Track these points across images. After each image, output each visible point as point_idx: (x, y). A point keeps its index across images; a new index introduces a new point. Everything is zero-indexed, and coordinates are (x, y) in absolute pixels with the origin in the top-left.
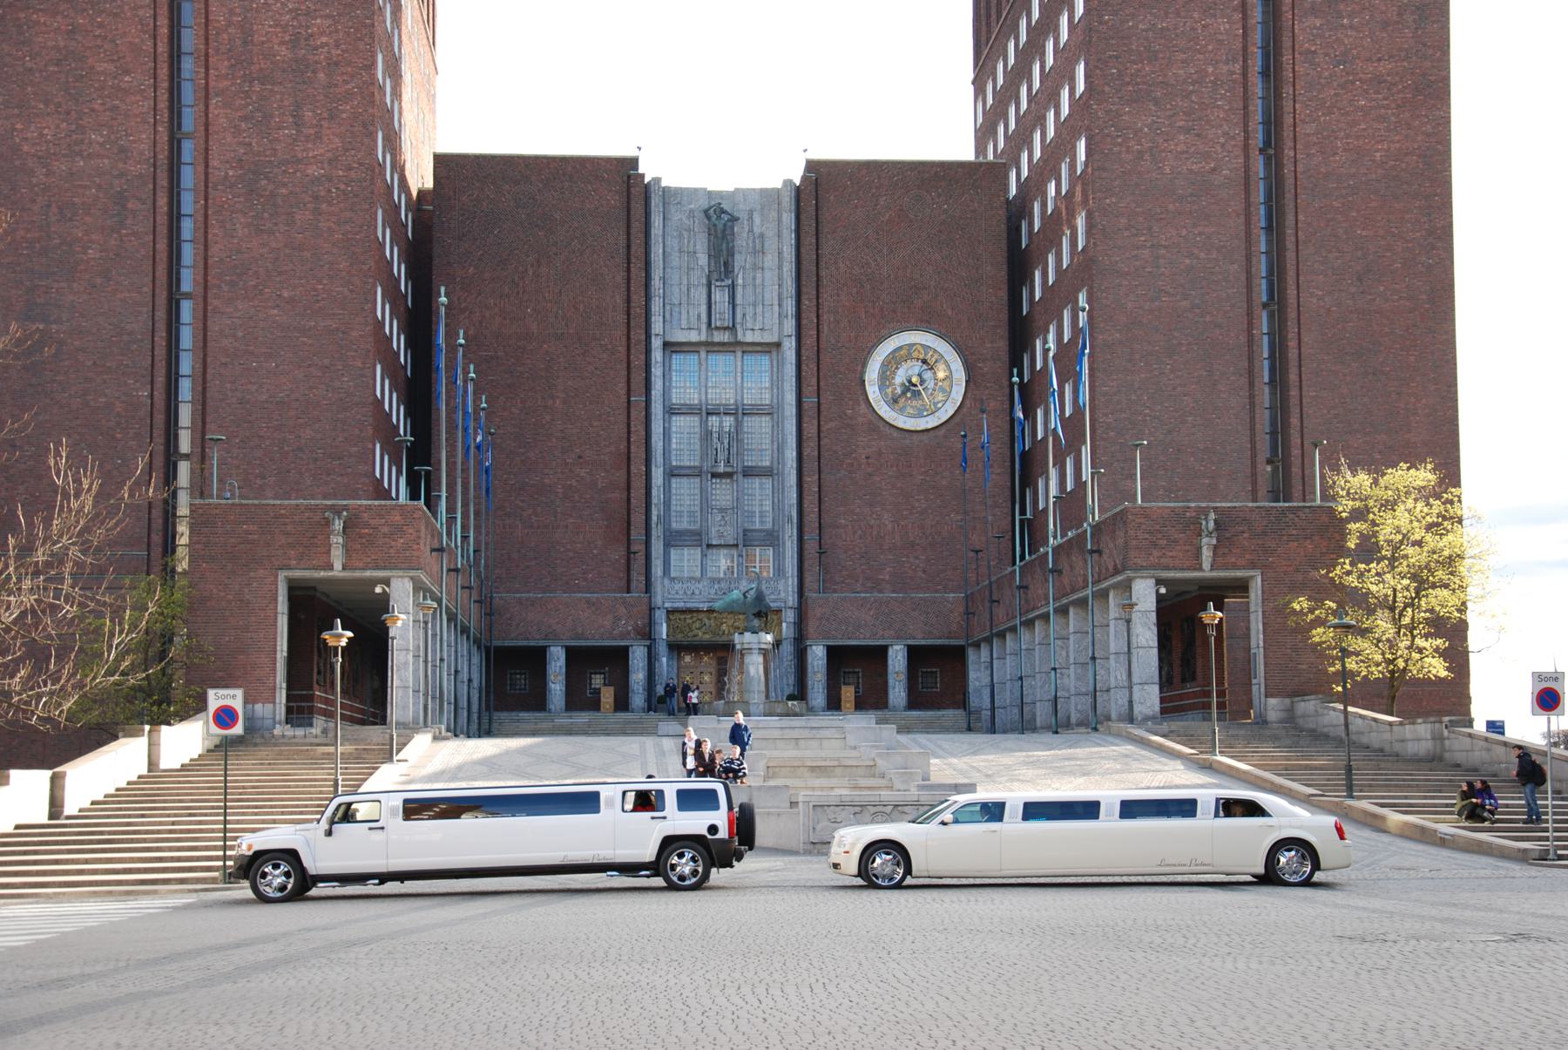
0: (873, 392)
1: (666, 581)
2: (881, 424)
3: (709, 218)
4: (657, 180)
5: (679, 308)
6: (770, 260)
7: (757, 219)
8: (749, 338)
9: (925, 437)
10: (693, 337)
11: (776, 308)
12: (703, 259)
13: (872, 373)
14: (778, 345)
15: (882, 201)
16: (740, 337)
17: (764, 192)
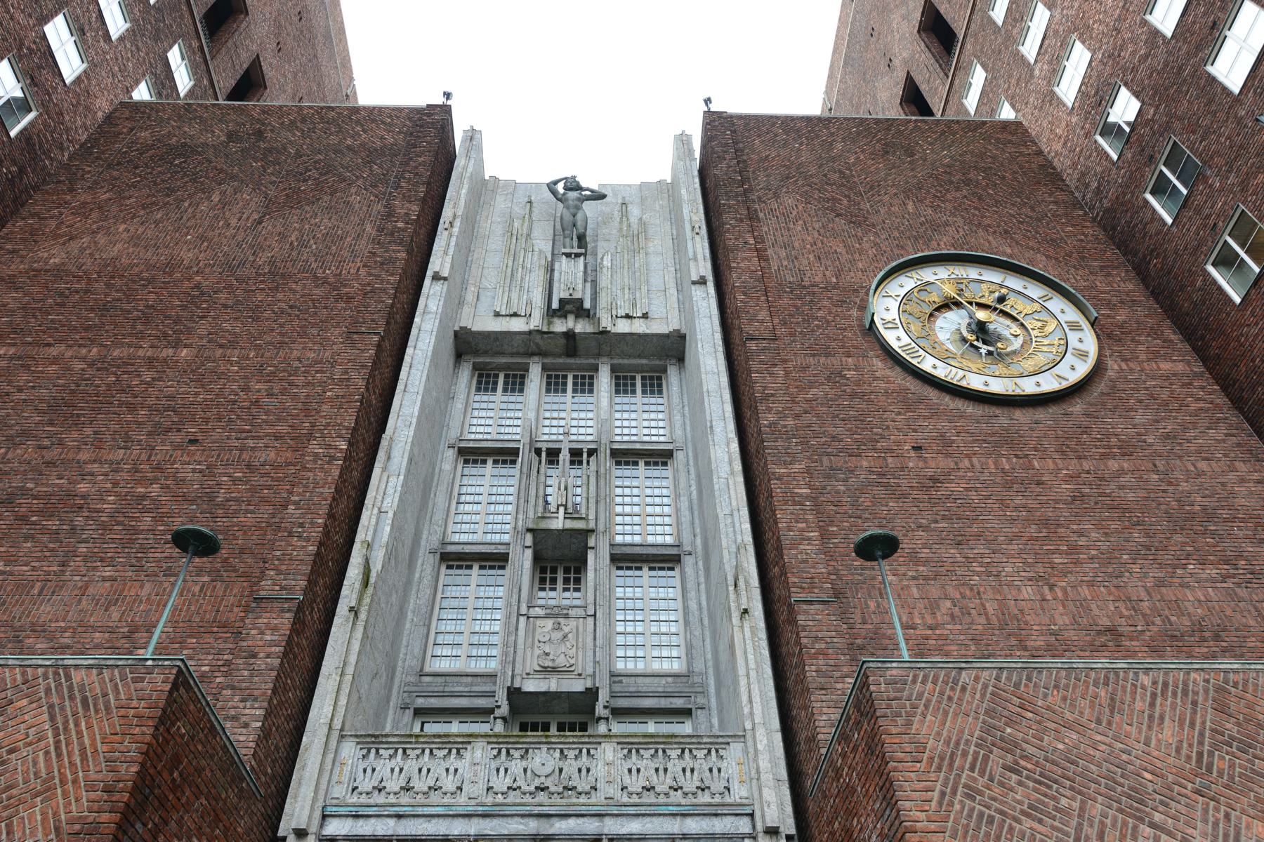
0: (896, 339)
1: (350, 750)
2: (932, 394)
3: (554, 193)
4: (473, 136)
5: (485, 281)
6: (659, 245)
7: (635, 212)
8: (623, 327)
9: (1042, 414)
10: (517, 325)
11: (673, 291)
12: (542, 243)
13: (886, 307)
14: (673, 349)
15: (839, 146)
16: (606, 323)
17: (643, 186)
